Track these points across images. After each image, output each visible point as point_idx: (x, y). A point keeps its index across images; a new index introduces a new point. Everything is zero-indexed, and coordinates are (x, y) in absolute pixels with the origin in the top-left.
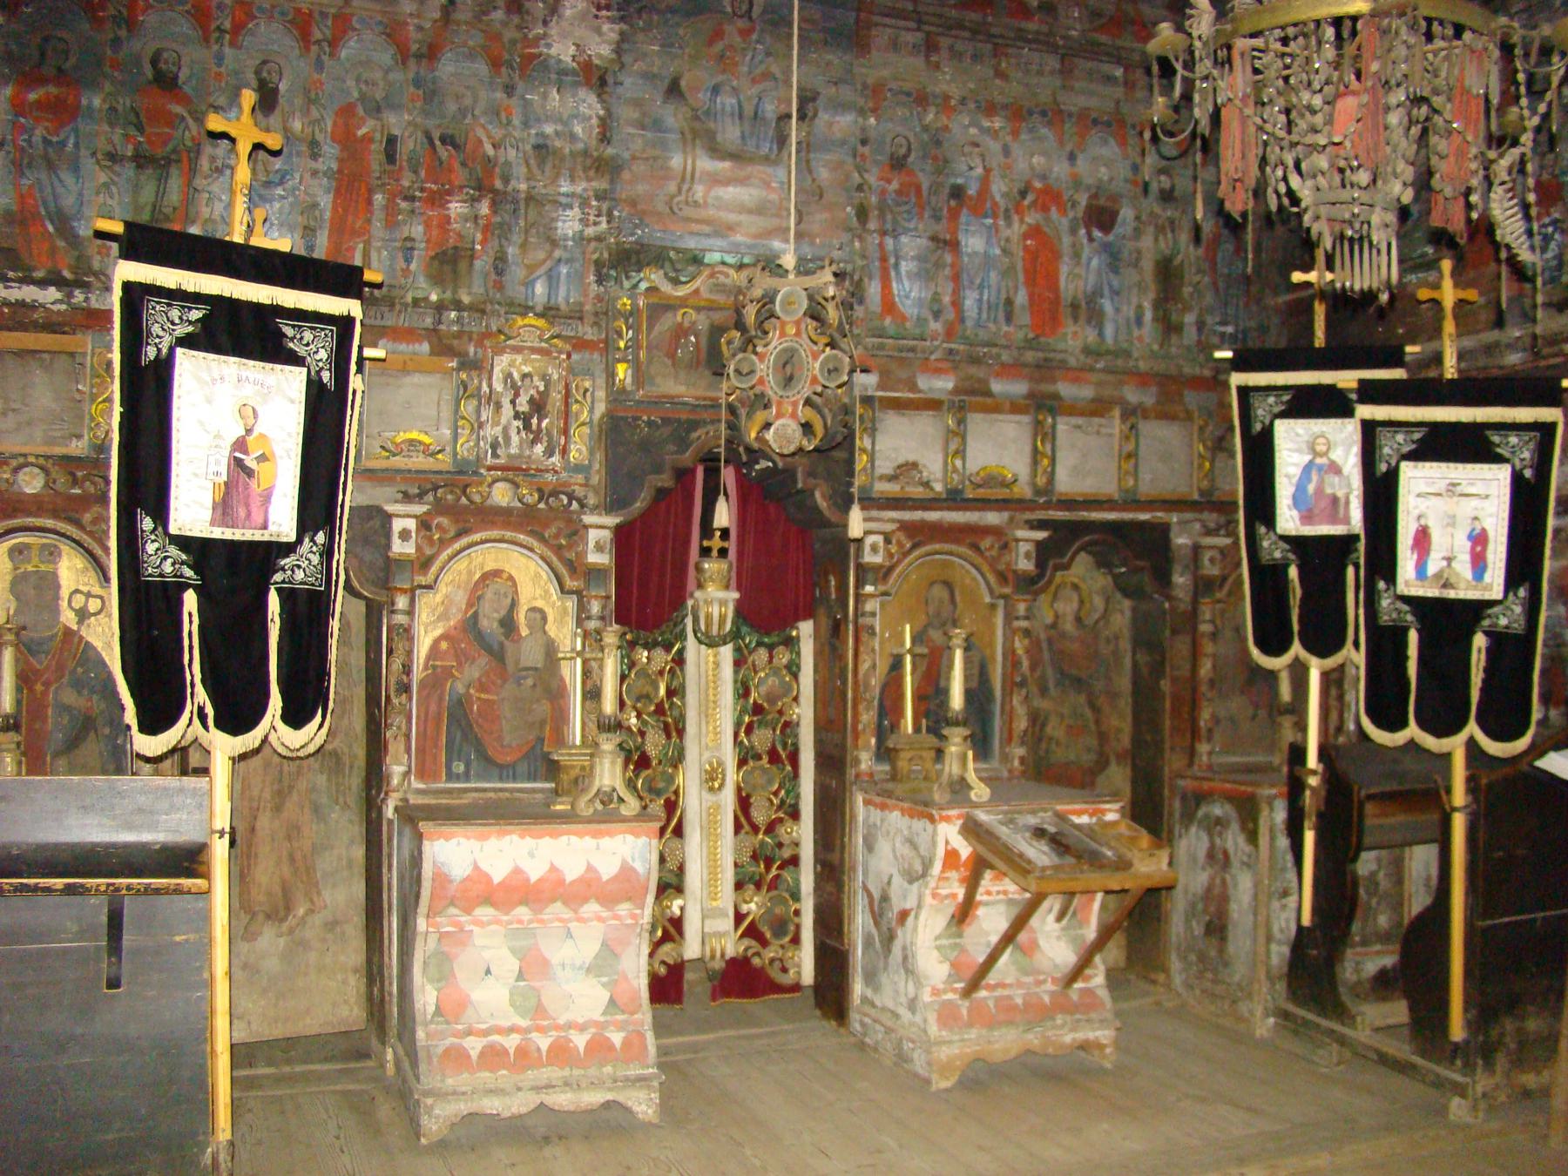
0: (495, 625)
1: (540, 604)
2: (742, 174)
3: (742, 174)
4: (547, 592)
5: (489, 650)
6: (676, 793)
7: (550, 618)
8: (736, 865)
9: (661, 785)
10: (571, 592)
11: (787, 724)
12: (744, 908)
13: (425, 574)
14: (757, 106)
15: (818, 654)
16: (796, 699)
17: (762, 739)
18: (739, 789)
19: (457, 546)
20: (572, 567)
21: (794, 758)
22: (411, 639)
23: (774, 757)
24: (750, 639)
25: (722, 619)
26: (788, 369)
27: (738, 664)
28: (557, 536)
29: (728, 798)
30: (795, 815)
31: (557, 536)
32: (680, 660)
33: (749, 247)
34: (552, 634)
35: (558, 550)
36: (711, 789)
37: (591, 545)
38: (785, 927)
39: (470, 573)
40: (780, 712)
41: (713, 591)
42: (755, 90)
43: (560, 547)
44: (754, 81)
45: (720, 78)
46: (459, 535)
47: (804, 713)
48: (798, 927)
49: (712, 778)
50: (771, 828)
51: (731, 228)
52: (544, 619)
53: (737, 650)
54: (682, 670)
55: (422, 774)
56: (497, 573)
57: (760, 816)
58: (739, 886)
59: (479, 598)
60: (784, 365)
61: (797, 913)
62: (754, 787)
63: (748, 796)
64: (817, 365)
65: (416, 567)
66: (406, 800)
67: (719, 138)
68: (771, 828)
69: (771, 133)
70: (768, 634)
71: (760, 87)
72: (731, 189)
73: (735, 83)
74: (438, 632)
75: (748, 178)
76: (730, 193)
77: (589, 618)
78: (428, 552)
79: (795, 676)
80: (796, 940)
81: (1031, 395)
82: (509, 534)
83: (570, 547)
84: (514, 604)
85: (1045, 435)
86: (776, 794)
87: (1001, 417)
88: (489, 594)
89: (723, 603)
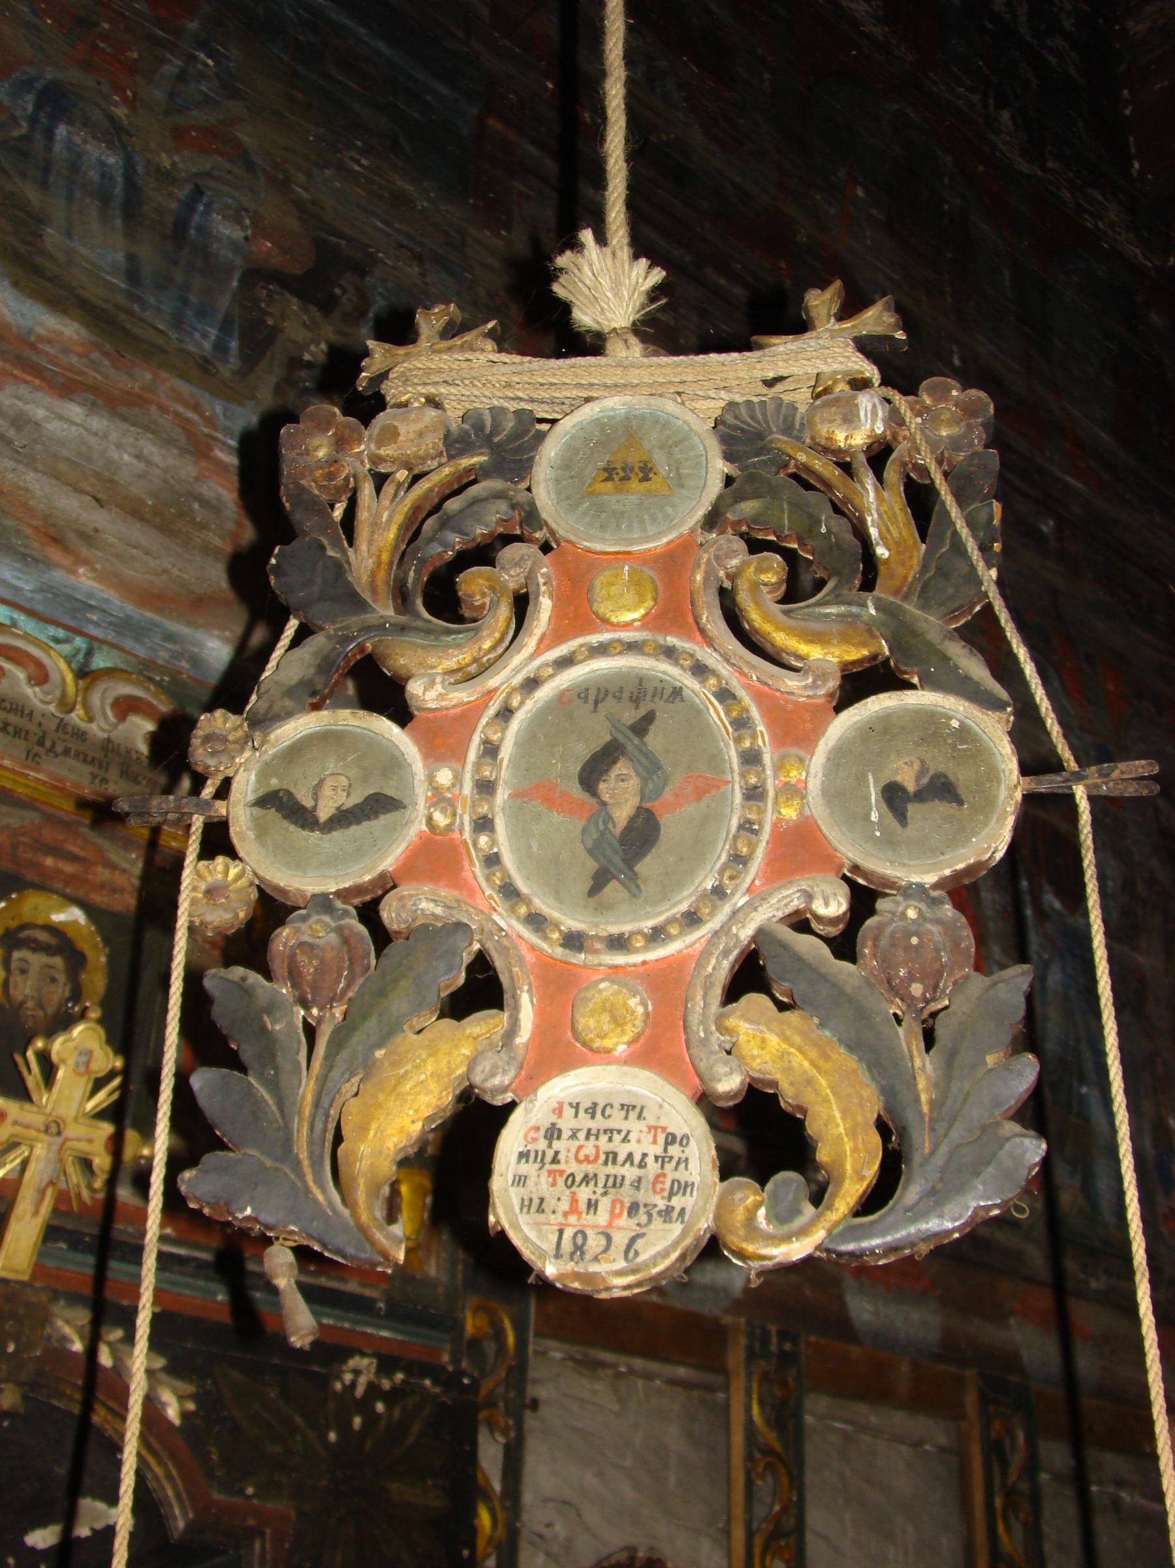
2: (122, 381)
3: (122, 381)
14: (189, 206)
26: (622, 792)
33: (125, 626)
42: (186, 162)
44: (179, 135)
45: (73, 76)
51: (58, 535)
60: (592, 774)
64: (814, 770)
67: (52, 236)
69: (224, 302)
71: (207, 163)
72: (75, 411)
73: (121, 112)
75: (136, 400)
76: (67, 421)
81: (952, 1349)
85: (1010, 1493)
87: (874, 1417)
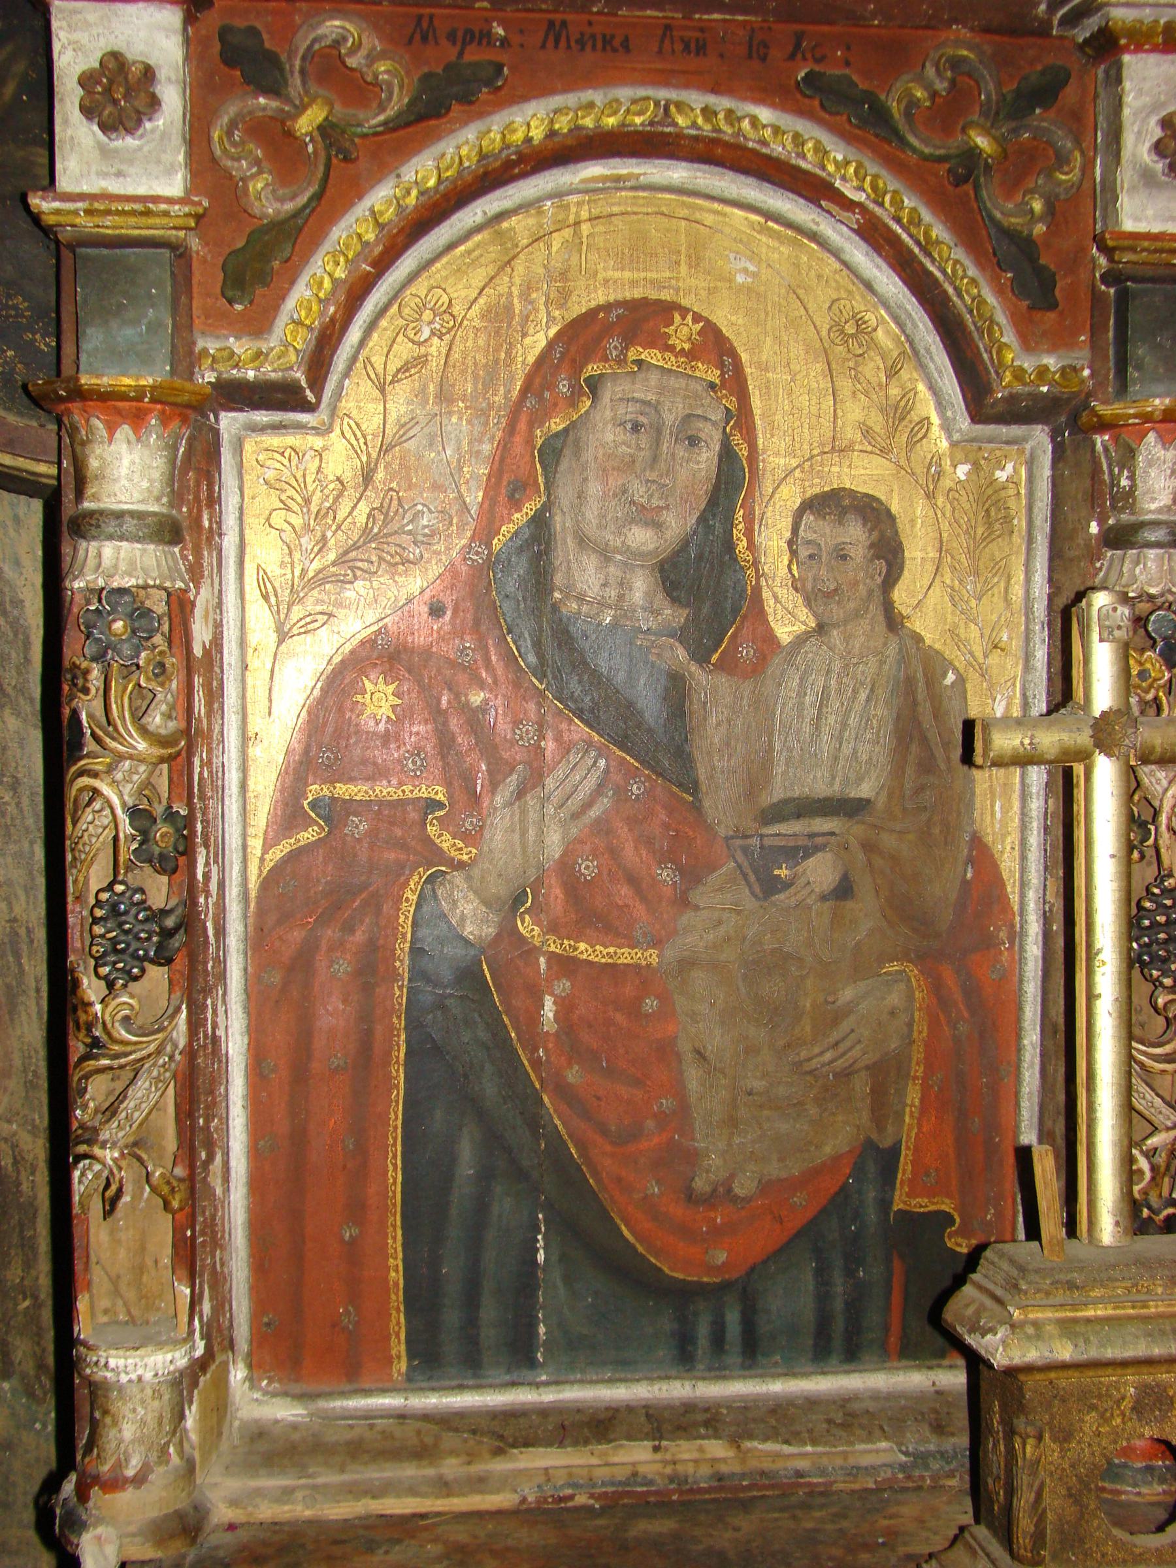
0: (641, 586)
1: (863, 474)
4: (898, 412)
5: (614, 719)
7: (917, 552)
10: (1018, 412)
13: (258, 324)
19: (424, 170)
20: (1033, 278)
22: (201, 671)
28: (948, 112)
31: (948, 112)
34: (926, 626)
35: (956, 184)
37: (1139, 142)
39: (502, 321)
43: (968, 166)
46: (428, 113)
52: (889, 553)
55: (296, 1345)
56: (642, 320)
59: (552, 453)
65: (207, 277)
66: (187, 1525)
74: (352, 626)
77: (1121, 538)
78: (266, 196)
82: (694, 108)
83: (1021, 164)
84: (732, 481)
88: (606, 434)
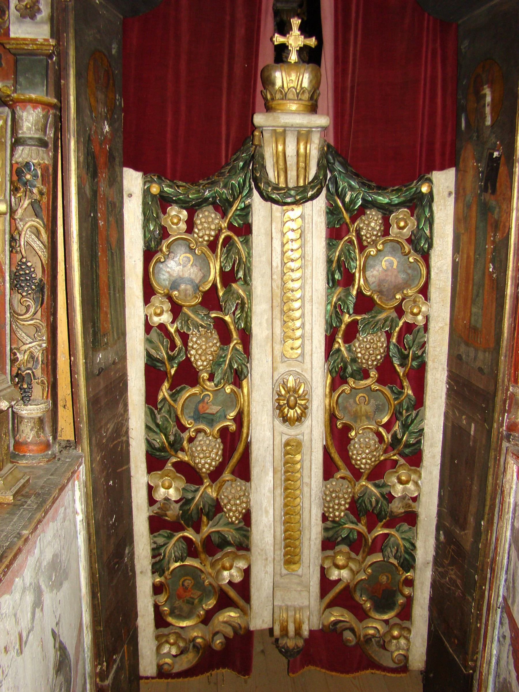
6: (239, 419)
8: (325, 518)
9: (214, 409)
11: (409, 328)
12: (334, 575)
15: (460, 220)
16: (424, 291)
17: (370, 347)
18: (332, 418)
21: (418, 377)
23: (386, 374)
24: (353, 193)
25: (303, 159)
27: (335, 233)
29: (314, 432)
30: (415, 459)
32: (245, 230)
36: (285, 419)
38: (388, 595)
40: (400, 311)
41: (292, 116)
47: (438, 312)
48: (410, 600)
49: (289, 405)
50: (377, 473)
53: (332, 212)
54: (247, 243)
57: (364, 450)
58: (328, 544)
61: (410, 583)
62: (356, 417)
63: (347, 428)
68: (377, 473)
70: (381, 188)
79: (426, 257)
80: (406, 613)
86: (388, 426)
89: (304, 135)
